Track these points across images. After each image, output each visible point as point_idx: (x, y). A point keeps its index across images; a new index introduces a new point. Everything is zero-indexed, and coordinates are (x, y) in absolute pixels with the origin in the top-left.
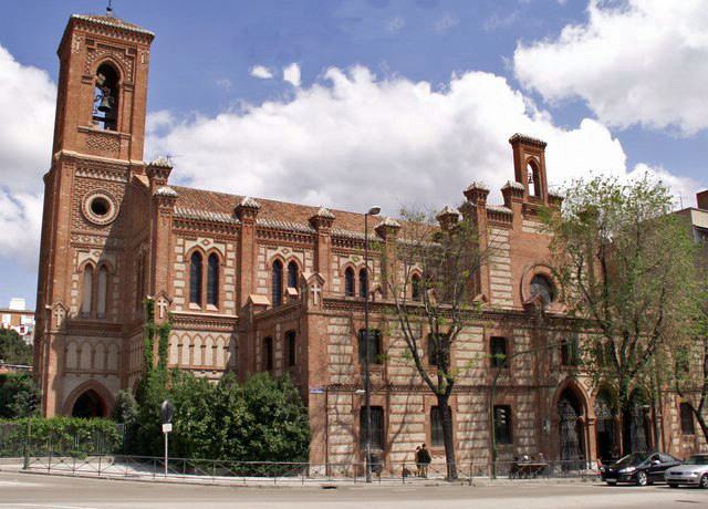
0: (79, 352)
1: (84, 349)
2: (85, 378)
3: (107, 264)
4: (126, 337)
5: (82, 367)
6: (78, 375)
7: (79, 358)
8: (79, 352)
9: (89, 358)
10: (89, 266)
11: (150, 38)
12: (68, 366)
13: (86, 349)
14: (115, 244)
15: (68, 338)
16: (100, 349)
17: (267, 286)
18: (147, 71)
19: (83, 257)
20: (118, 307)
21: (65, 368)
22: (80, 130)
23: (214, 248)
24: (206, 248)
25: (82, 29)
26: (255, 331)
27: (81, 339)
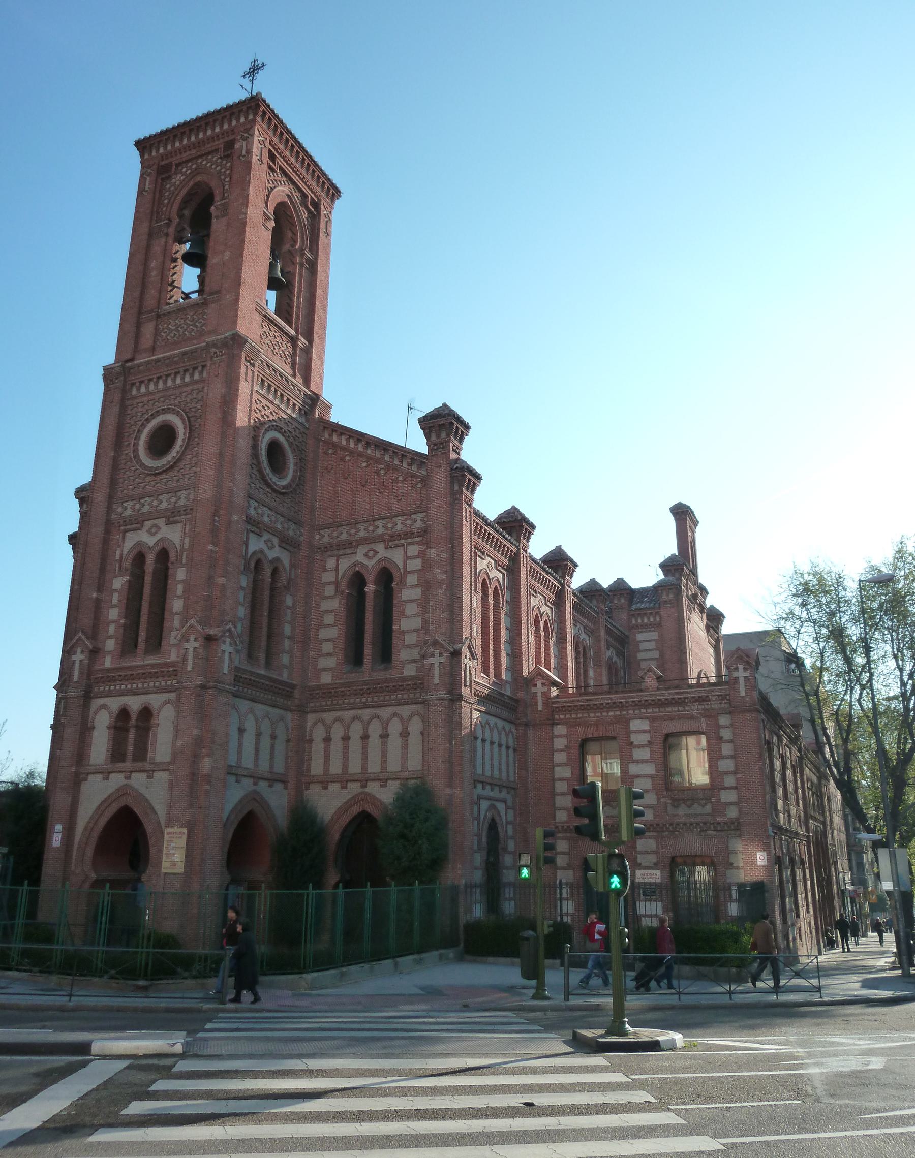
0: (241, 731)
4: (302, 711)
8: (241, 731)
9: (254, 742)
13: (250, 725)
16: (266, 727)
18: (328, 246)
19: (255, 544)
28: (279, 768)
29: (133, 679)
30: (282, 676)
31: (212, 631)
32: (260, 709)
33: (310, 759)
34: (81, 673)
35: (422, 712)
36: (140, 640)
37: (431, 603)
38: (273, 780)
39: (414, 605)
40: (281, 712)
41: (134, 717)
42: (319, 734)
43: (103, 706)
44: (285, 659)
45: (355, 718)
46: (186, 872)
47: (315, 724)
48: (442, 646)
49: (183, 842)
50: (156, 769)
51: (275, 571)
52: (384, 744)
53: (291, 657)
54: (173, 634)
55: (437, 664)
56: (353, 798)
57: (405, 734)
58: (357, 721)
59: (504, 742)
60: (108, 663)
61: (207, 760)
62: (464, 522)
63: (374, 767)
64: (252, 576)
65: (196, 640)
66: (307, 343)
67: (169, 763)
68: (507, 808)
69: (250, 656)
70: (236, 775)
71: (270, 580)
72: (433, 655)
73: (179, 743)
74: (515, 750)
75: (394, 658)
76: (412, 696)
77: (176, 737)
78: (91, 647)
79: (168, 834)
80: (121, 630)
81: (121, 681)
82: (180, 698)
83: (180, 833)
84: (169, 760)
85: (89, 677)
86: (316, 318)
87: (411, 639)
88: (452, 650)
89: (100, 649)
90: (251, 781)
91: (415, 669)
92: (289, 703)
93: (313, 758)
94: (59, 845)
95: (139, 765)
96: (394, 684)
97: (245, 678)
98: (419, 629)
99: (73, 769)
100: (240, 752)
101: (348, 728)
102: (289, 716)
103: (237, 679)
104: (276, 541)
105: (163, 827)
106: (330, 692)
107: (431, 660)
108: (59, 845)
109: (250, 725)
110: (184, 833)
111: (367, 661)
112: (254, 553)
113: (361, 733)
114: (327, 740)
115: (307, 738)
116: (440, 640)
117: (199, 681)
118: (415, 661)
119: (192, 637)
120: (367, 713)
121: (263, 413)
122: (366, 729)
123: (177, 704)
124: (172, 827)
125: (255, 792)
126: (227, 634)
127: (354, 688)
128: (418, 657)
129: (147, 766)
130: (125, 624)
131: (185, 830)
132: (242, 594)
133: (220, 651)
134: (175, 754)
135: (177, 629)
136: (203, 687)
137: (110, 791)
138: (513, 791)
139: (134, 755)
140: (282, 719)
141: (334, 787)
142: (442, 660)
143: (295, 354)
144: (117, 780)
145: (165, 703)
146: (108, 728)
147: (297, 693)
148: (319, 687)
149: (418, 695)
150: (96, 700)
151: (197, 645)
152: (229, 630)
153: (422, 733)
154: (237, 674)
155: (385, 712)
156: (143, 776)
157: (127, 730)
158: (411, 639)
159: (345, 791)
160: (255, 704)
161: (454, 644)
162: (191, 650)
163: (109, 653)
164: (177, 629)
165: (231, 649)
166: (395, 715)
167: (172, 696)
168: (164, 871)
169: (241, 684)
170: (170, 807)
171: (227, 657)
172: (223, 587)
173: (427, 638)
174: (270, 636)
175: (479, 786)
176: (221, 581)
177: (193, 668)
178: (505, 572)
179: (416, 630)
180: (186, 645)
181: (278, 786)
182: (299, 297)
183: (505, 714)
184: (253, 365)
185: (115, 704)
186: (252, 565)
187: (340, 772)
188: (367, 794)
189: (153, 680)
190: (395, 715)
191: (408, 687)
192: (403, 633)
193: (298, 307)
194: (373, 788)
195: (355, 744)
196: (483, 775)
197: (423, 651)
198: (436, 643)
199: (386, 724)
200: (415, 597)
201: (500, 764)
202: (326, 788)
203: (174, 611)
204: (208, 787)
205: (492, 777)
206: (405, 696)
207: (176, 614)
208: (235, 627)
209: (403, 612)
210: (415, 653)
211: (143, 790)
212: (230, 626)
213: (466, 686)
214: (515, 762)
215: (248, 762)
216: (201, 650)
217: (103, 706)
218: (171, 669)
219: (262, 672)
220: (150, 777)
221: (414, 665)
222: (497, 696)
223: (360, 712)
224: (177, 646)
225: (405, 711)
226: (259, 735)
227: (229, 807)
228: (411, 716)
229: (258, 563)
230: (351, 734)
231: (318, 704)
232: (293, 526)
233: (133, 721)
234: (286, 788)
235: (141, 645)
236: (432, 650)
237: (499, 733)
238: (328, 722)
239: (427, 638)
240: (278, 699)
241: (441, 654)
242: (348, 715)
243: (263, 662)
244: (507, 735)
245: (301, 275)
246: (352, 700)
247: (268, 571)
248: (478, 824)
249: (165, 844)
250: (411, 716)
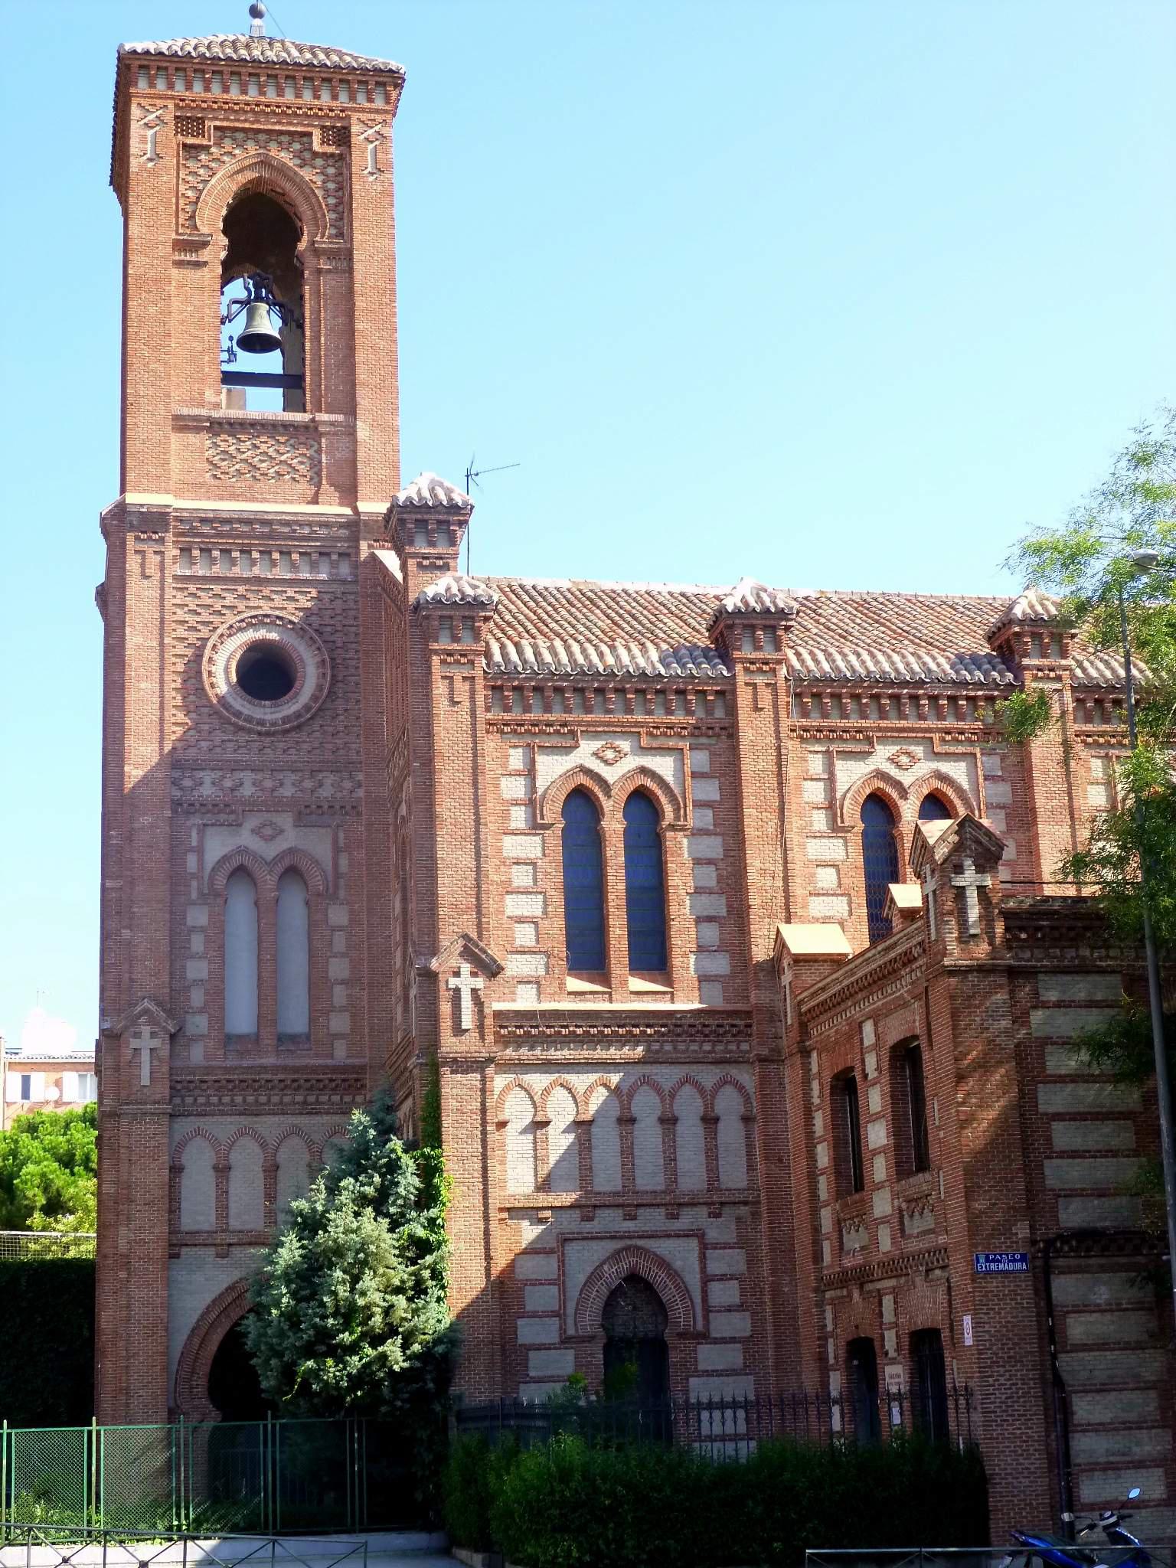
0: (223, 1171)
1: (235, 1157)
3: (303, 864)
5: (234, 1223)
6: (224, 1250)
7: (223, 1194)
8: (223, 1171)
10: (241, 872)
11: (387, 81)
12: (187, 1222)
14: (326, 792)
15: (184, 1126)
17: (840, 890)
18: (388, 194)
19: (217, 846)
21: (174, 1230)
22: (183, 424)
23: (644, 771)
24: (611, 774)
25: (161, 85)
26: (805, 1053)
27: (224, 1127)
30: (332, 1057)
32: (270, 1125)
62: (441, 705)
66: (340, 418)
68: (704, 1247)
86: (359, 357)
104: (285, 820)
112: (225, 859)
121: (218, 607)
143: (319, 451)
176: (126, 933)
178: (685, 745)
182: (316, 338)
184: (162, 540)
193: (317, 356)
213: (458, 1030)
219: (270, 1060)
232: (329, 779)
245: (317, 293)
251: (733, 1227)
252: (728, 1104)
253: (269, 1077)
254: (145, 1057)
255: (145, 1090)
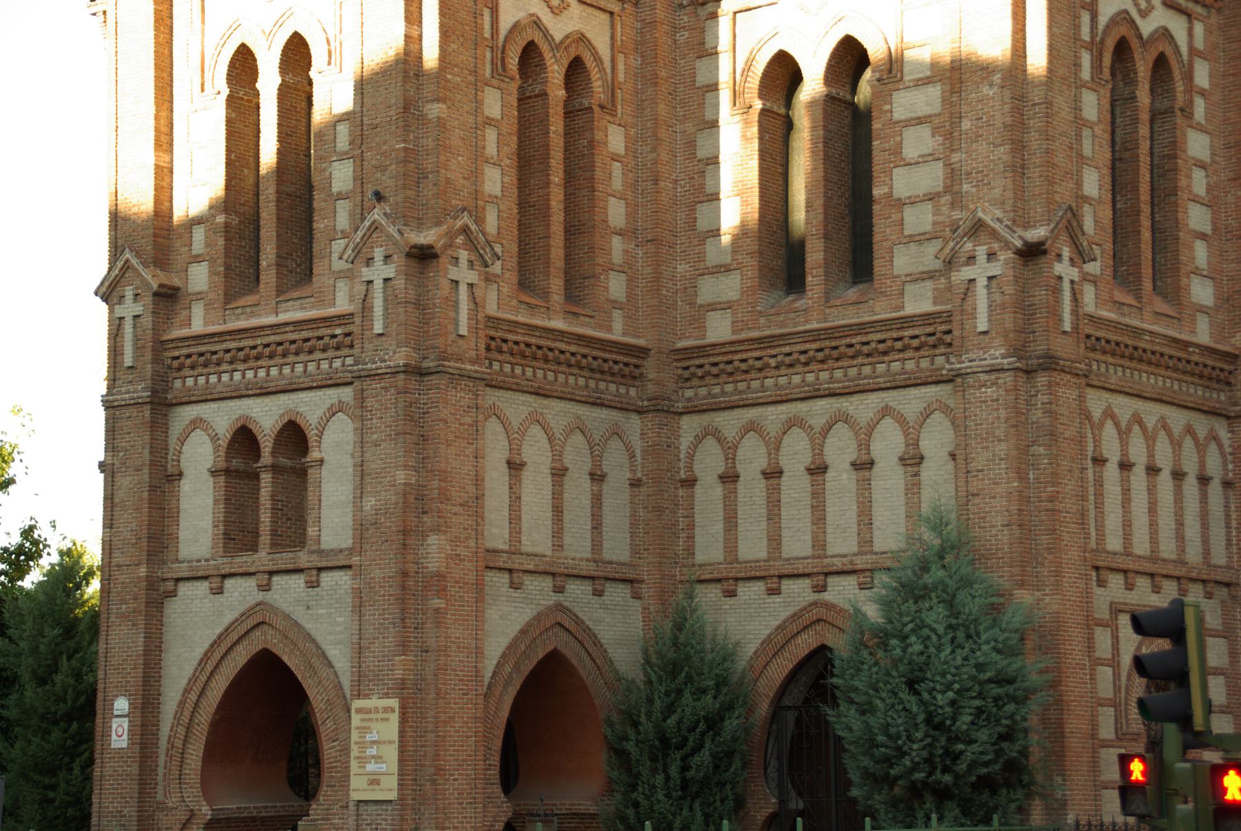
0: (515, 467)
2: (540, 591)
8: (515, 467)
13: (537, 452)
16: (577, 456)
20: (628, 269)
27: (517, 406)
28: (617, 548)
29: (257, 358)
30: (609, 329)
31: (426, 237)
32: (559, 413)
33: (691, 526)
34: (138, 349)
35: (951, 403)
36: (264, 263)
37: (966, 125)
38: (599, 580)
39: (925, 131)
40: (615, 415)
41: (267, 446)
42: (709, 462)
43: (197, 423)
44: (616, 286)
45: (792, 423)
46: (402, 797)
47: (699, 439)
48: (994, 234)
49: (391, 728)
50: (324, 564)
51: (575, 70)
52: (865, 487)
53: (631, 280)
54: (338, 245)
55: (982, 282)
56: (795, 616)
57: (913, 460)
58: (796, 430)
59: (1190, 466)
60: (199, 321)
61: (432, 539)
63: (842, 543)
64: (513, 87)
65: (387, 258)
67: (351, 551)
69: (525, 284)
70: (510, 571)
71: (562, 93)
72: (971, 259)
73: (369, 503)
74: (1227, 484)
75: (879, 266)
76: (925, 364)
77: (360, 491)
78: (155, 287)
79: (359, 711)
80: (221, 242)
81: (231, 363)
82: (363, 399)
83: (387, 710)
84: (349, 543)
85: (156, 360)
87: (919, 219)
88: (1019, 243)
89: (177, 289)
90: (547, 583)
91: (930, 294)
92: (633, 392)
93: (698, 519)
94: (125, 745)
95: (285, 559)
96: (879, 336)
97: (516, 343)
98: (938, 194)
99: (143, 571)
100: (515, 519)
101: (778, 449)
102: (634, 425)
103: (494, 346)
105: (348, 696)
106: (730, 362)
107: (967, 272)
108: (125, 745)
109: (537, 452)
110: (393, 710)
111: (814, 279)
112: (516, 27)
113: (806, 458)
114: (730, 478)
115: (683, 475)
116: (987, 219)
117: (400, 358)
118: (931, 275)
119: (378, 253)
120: (820, 409)
122: (818, 447)
123: (360, 411)
124: (367, 696)
125: (559, 607)
126: (460, 240)
127: (787, 349)
128: (938, 264)
129: (304, 558)
130: (227, 225)
131: (394, 703)
132: (491, 136)
133: (445, 284)
134: (361, 528)
135: (345, 235)
136: (417, 372)
137: (229, 617)
138: (1223, 592)
139: (274, 533)
140: (617, 433)
141: (750, 592)
142: (995, 269)
144: (241, 593)
145: (332, 412)
146: (214, 473)
147: (650, 368)
148: (701, 350)
149: (940, 360)
150: (180, 409)
151: (390, 271)
152: (465, 230)
153: (953, 456)
154: (492, 333)
155: (863, 407)
156: (298, 581)
157: (256, 476)
158: (919, 219)
159: (777, 599)
160: (546, 402)
161: (1026, 226)
162: (378, 284)
163: (199, 296)
164: (345, 235)
165: (473, 277)
166: (886, 411)
167: (347, 394)
168: (355, 796)
169: (507, 357)
170: (359, 651)
171: (463, 291)
172: (441, 123)
173: (957, 215)
174: (572, 231)
175: (1116, 581)
177: (386, 327)
179: (931, 197)
180: (366, 273)
181: (617, 594)
183: (1197, 393)
185: (223, 417)
186: (513, 62)
187: (763, 554)
188: (829, 606)
189: (302, 357)
190: (886, 411)
191: (915, 343)
192: (900, 204)
194: (842, 591)
195: (795, 486)
196: (1127, 553)
197: (947, 250)
198: (978, 228)
199: (865, 436)
200: (927, 111)
201: (1180, 524)
202: (731, 594)
203: (335, 190)
204: (437, 603)
205: (1154, 558)
206: (910, 365)
207: (341, 196)
208: (480, 221)
209: (898, 151)
210: (928, 256)
211: (299, 615)
212: (466, 219)
214: (1228, 516)
215: (537, 539)
216: (400, 283)
217: (197, 423)
218: (338, 331)
219: (558, 324)
220: (313, 584)
221: (929, 284)
222: (1167, 351)
223: (802, 407)
224: (349, 275)
225: (911, 401)
226: (559, 473)
227: (495, 648)
228: (926, 415)
229: (530, 54)
230: (784, 463)
231: (703, 391)
233: (266, 458)
234: (637, 596)
235: (269, 277)
236: (969, 246)
237: (1177, 445)
238: (730, 433)
239: (957, 215)
240: (602, 385)
241: (991, 256)
242: (773, 416)
243: (557, 298)
244: (1201, 448)
246: (783, 381)
247: (555, 71)
248: (1117, 676)
249: (355, 736)
250: (926, 415)
251: (1220, 612)
252: (1214, 465)
253: (562, 346)
254: (463, 291)
255: (461, 342)
